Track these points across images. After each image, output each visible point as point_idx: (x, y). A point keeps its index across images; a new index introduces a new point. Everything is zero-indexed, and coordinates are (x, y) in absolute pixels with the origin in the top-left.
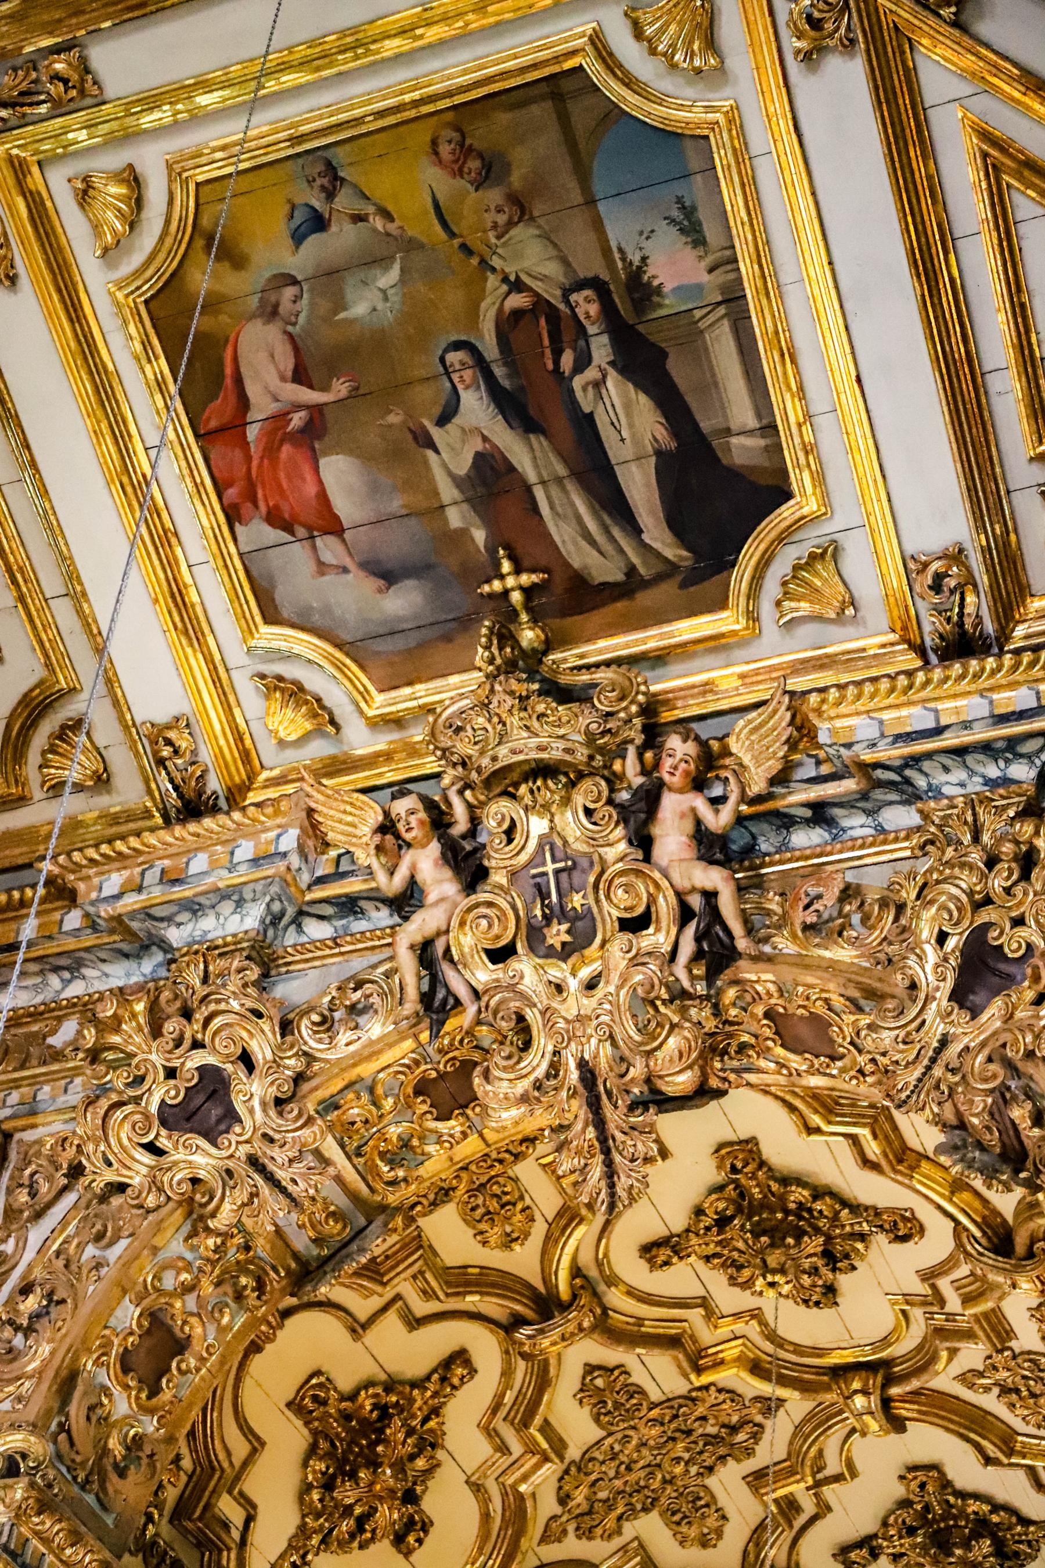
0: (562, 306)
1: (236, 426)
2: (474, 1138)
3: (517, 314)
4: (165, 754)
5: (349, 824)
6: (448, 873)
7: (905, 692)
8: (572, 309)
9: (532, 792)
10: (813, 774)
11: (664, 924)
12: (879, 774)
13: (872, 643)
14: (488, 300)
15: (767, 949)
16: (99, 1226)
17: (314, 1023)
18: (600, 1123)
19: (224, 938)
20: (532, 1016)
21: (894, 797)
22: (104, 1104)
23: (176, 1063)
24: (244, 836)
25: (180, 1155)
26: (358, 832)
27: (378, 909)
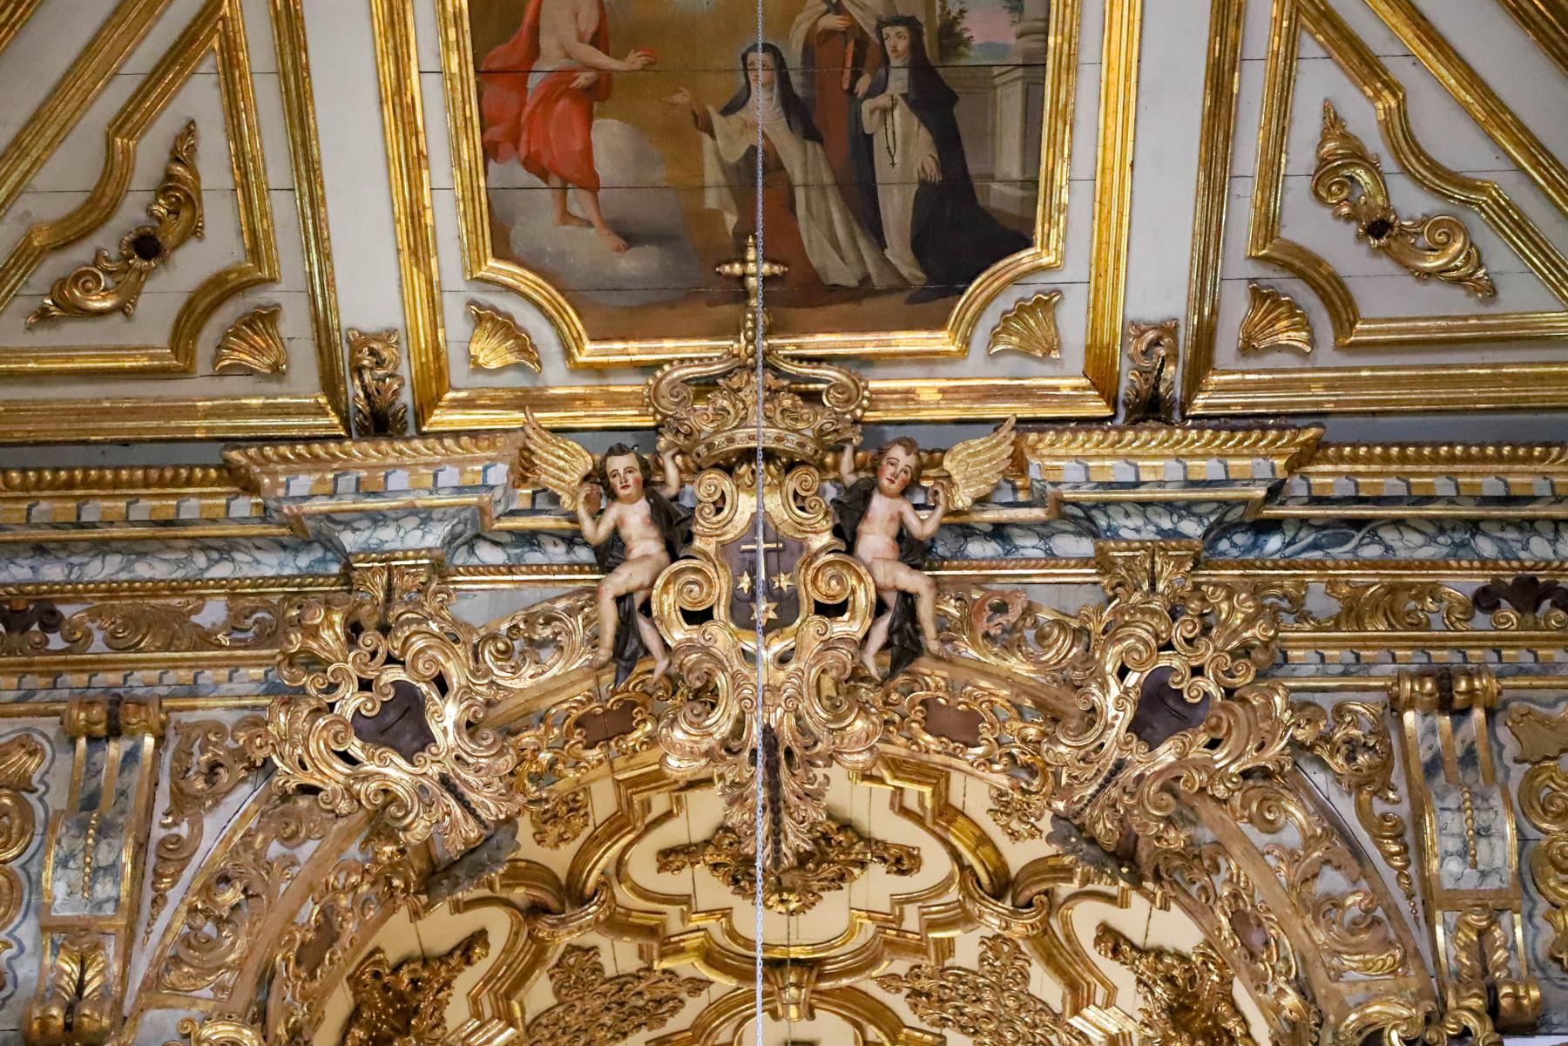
0: (873, 36)
1: (517, 74)
2: (606, 764)
3: (830, 33)
4: (366, 362)
5: (560, 469)
6: (653, 533)
7: (1112, 445)
8: (882, 41)
9: (753, 472)
10: (1010, 499)
11: (860, 613)
13: (1066, 384)
14: (806, 14)
15: (948, 647)
16: (293, 827)
17: (498, 651)
19: (405, 551)
20: (721, 680)
21: (1069, 527)
23: (371, 675)
24: (450, 462)
25: (370, 767)
26: (567, 478)
27: (555, 544)
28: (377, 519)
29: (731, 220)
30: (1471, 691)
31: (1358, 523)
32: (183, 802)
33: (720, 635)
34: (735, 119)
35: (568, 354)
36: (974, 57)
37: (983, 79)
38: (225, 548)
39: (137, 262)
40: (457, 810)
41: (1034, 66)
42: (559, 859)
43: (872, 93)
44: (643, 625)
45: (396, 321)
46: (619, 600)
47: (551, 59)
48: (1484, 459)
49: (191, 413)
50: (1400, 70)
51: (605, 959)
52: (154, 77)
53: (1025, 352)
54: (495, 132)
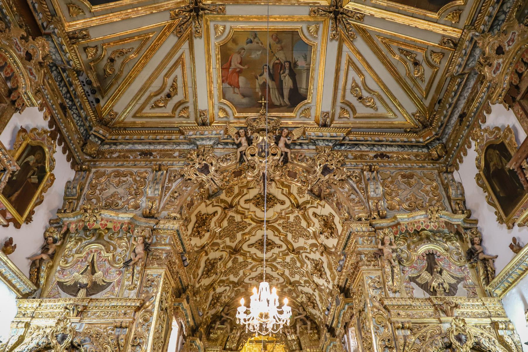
3: (277, 63)
12: (312, 141)
13: (311, 122)
18: (264, 182)
20: (256, 165)
22: (189, 166)
28: (203, 139)
29: (260, 94)
30: (374, 168)
31: (356, 145)
32: (170, 181)
33: (256, 158)
34: (261, 77)
35: (234, 115)
36: (299, 68)
37: (300, 72)
38: (179, 144)
39: (167, 98)
40: (213, 184)
41: (308, 70)
42: (229, 200)
43: (284, 73)
44: (244, 156)
45: (207, 108)
46: (241, 152)
47: (233, 66)
48: (376, 135)
49: (175, 123)
50: (364, 72)
51: (236, 219)
52: (171, 68)
53: (305, 117)
54: (224, 78)
